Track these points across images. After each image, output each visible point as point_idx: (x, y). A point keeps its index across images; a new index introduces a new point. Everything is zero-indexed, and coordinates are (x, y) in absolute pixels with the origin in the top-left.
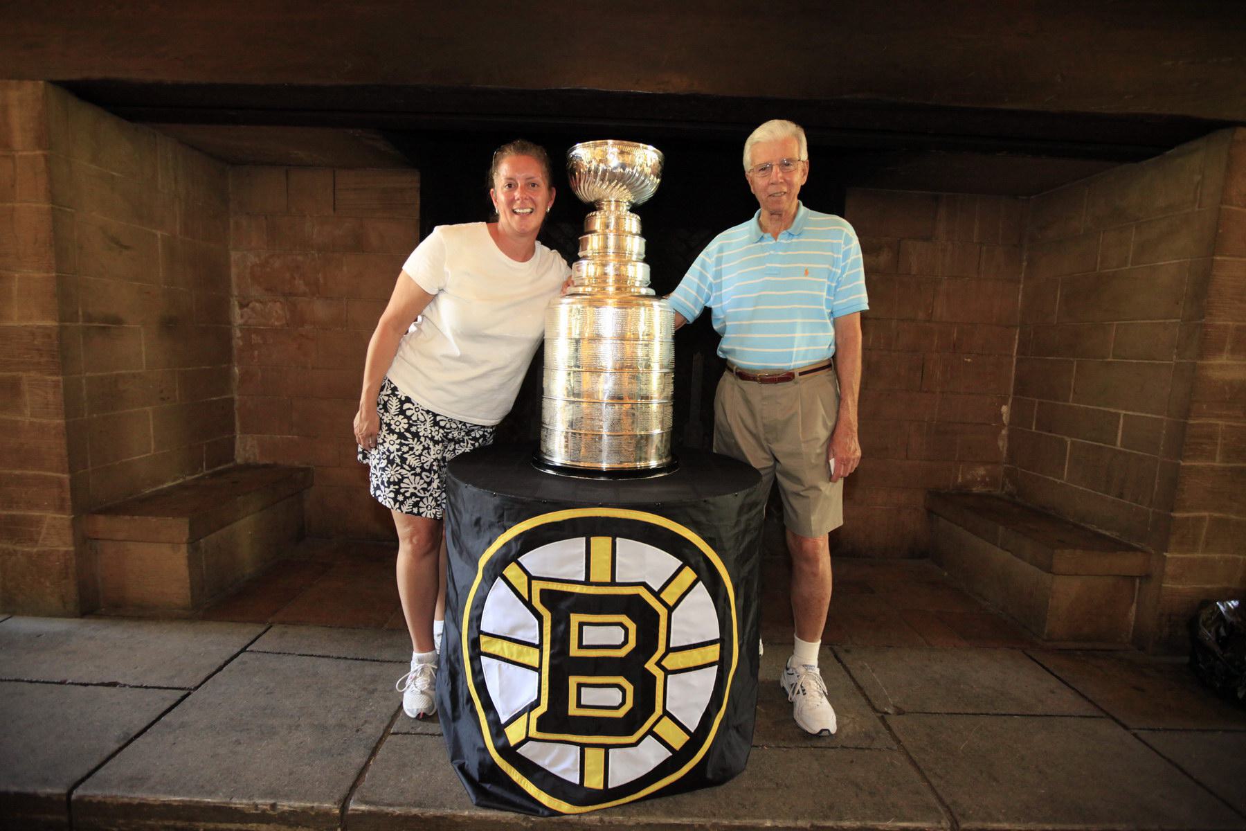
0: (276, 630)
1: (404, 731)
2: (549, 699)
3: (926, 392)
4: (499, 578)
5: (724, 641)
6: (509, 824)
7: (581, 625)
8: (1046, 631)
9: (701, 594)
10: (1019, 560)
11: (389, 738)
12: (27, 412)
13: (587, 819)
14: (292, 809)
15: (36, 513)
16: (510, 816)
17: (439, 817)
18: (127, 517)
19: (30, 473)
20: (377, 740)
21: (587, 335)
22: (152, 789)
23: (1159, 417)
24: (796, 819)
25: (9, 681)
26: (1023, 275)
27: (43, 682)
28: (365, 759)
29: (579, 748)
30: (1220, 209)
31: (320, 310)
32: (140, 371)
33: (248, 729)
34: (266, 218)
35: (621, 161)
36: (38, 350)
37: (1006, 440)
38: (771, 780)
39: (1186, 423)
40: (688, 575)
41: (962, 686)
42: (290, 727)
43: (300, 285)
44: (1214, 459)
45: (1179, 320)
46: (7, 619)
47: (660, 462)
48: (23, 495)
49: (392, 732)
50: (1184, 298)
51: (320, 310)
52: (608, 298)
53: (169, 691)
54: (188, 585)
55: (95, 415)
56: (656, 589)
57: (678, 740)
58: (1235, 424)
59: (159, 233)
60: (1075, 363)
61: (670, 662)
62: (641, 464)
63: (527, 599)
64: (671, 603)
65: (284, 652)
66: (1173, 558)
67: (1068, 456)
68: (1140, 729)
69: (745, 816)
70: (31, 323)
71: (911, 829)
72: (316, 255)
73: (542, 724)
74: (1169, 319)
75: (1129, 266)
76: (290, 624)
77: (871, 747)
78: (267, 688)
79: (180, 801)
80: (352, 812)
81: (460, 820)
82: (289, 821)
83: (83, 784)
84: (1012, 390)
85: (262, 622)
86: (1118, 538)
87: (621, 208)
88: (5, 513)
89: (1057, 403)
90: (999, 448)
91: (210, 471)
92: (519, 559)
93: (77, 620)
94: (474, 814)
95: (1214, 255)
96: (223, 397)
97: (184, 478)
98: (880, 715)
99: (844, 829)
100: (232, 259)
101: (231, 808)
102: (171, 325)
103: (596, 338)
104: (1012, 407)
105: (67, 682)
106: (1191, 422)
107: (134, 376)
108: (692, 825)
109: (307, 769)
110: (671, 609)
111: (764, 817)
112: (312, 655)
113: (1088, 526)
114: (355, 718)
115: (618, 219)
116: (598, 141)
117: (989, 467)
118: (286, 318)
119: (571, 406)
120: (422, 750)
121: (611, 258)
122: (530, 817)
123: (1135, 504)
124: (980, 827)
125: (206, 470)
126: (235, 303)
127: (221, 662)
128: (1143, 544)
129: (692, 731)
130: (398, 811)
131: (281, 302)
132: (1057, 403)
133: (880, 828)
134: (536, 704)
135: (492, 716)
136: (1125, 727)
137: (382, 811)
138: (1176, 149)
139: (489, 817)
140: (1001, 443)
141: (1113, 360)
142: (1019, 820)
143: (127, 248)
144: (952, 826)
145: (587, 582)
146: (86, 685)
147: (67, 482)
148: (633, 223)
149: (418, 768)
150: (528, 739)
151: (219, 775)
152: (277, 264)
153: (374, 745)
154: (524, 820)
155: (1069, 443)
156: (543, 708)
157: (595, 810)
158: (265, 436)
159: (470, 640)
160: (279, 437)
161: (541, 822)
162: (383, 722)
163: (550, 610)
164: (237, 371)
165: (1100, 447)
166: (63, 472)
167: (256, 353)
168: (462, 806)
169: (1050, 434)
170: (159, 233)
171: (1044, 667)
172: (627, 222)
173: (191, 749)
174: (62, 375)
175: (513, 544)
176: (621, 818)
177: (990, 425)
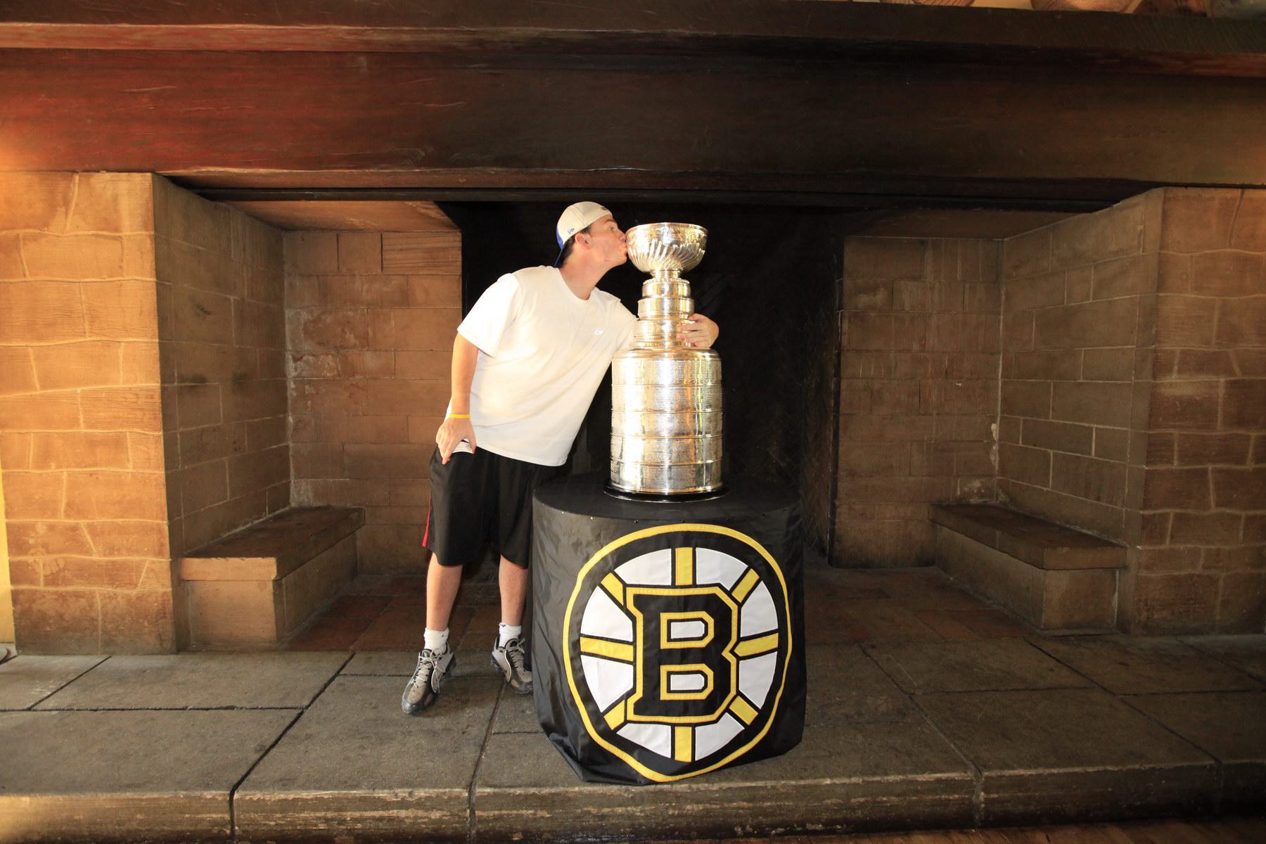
0: (360, 656)
1: (503, 732)
2: (644, 686)
3: (924, 415)
4: (598, 588)
5: (781, 631)
6: (612, 795)
7: (670, 622)
8: (1043, 621)
9: (763, 592)
10: (1017, 560)
11: (493, 737)
12: (130, 465)
13: (678, 787)
14: (427, 795)
15: (136, 558)
16: (614, 789)
17: (553, 794)
18: (222, 560)
19: (133, 520)
20: (483, 738)
21: (650, 383)
22: (304, 787)
23: (1125, 429)
24: (850, 777)
25: (134, 709)
26: (1002, 306)
27: (167, 709)
28: (478, 754)
29: (669, 727)
30: (1160, 253)
31: (370, 360)
32: (218, 425)
33: (367, 737)
34: (318, 276)
35: (674, 239)
36: (141, 409)
37: (997, 455)
38: (825, 750)
39: (1145, 433)
40: (753, 576)
41: (975, 670)
42: (403, 733)
43: (351, 338)
44: (1172, 464)
45: (1134, 346)
46: (105, 660)
47: (713, 487)
48: (125, 542)
49: (493, 732)
50: (1137, 328)
51: (370, 360)
52: (667, 352)
53: (284, 710)
54: (273, 620)
55: (186, 467)
56: (729, 589)
57: (749, 715)
58: (1185, 433)
59: (232, 298)
60: (1052, 384)
61: (742, 649)
62: (701, 489)
63: (621, 602)
64: (740, 601)
65: (376, 673)
66: (1146, 550)
67: (1051, 468)
68: (1125, 695)
69: (808, 778)
70: (135, 385)
71: (943, 778)
72: (366, 310)
73: (640, 708)
74: (1127, 345)
75: (1091, 301)
76: (371, 650)
77: (905, 721)
78: (371, 704)
79: (330, 794)
80: (480, 794)
81: (570, 796)
82: (425, 806)
83: (241, 786)
84: (999, 410)
85: (345, 650)
86: (1098, 536)
87: (674, 276)
88: (107, 559)
89: (1039, 420)
90: (991, 463)
91: (271, 515)
92: (616, 570)
93: (175, 656)
94: (582, 789)
95: (1158, 292)
96: (281, 445)
97: (252, 522)
98: (907, 696)
99: (892, 782)
100: (286, 317)
101: (375, 797)
102: (241, 381)
103: (657, 386)
104: (1000, 426)
105: (191, 707)
106: (1151, 432)
107: (214, 430)
108: (766, 787)
109: (431, 764)
110: (740, 605)
111: (823, 777)
112: (401, 676)
113: (1072, 527)
114: (458, 723)
115: (673, 286)
116: (657, 224)
117: (983, 480)
118: (337, 369)
119: (645, 441)
120: (524, 744)
121: (666, 318)
122: (630, 787)
123: (1111, 506)
124: (999, 774)
125: (270, 512)
126: (289, 356)
127: (321, 685)
128: (1119, 540)
129: (760, 708)
130: (518, 791)
131: (332, 355)
132: (1039, 420)
133: (919, 779)
134: (633, 691)
135: (591, 707)
136: (1112, 693)
137: (505, 792)
138: (1121, 203)
139: (595, 791)
140: (992, 458)
141: (1085, 381)
142: (1030, 767)
143: (208, 313)
144: (976, 776)
145: (673, 586)
146: (207, 709)
147: (167, 528)
148: (683, 288)
149: (527, 758)
150: (626, 722)
151: (356, 773)
152: (329, 319)
153: (482, 743)
154: (627, 790)
155: (1052, 454)
156: (639, 694)
157: (684, 779)
158: (318, 480)
159: (571, 644)
160: (331, 480)
161: (641, 792)
162: (483, 725)
163: (641, 611)
164: (291, 420)
165: (1079, 457)
166: (163, 519)
167: (309, 402)
168: (572, 784)
169: (1039, 448)
170: (232, 298)
171: (1044, 652)
172: (680, 287)
173: (324, 755)
174: (164, 430)
175: (610, 558)
176: (706, 785)
177: (982, 441)
